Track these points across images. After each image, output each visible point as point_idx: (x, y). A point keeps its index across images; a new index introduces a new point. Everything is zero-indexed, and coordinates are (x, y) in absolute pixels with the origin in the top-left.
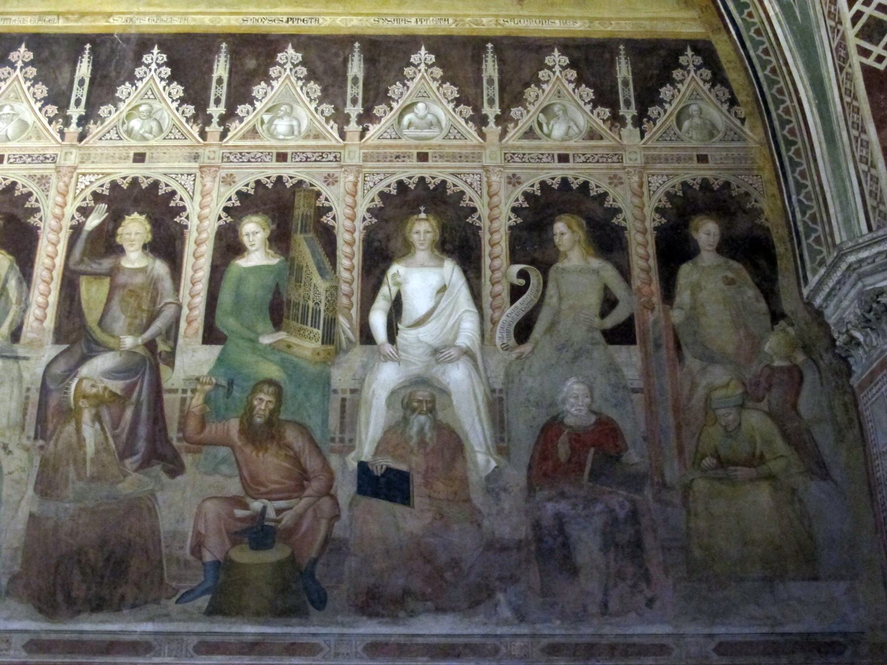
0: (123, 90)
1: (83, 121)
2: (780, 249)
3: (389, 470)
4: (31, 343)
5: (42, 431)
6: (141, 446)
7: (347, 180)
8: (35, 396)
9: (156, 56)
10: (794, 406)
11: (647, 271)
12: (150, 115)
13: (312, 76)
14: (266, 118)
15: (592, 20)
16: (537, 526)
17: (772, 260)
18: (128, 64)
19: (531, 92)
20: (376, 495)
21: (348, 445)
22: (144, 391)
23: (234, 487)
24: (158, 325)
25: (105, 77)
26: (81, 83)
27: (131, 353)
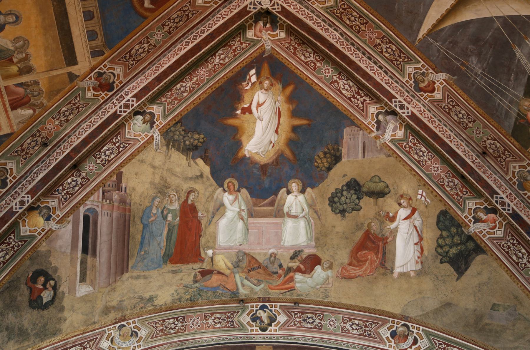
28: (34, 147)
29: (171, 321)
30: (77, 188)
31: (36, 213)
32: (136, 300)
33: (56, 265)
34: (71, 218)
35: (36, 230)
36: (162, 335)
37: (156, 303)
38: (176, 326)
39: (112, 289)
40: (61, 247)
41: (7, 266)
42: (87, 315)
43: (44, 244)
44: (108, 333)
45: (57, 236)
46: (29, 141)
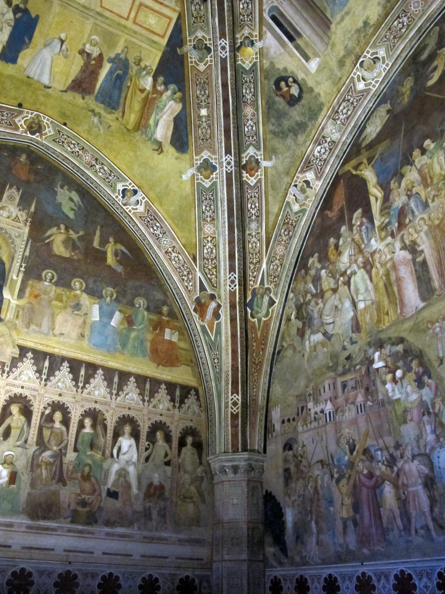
0: (57, 373)
1: (46, 380)
2: (204, 446)
3: (114, 491)
4: (30, 445)
5: (32, 470)
6: (57, 477)
7: (111, 411)
8: (30, 460)
9: (66, 364)
10: (201, 486)
11: (175, 448)
12: (64, 382)
13: (105, 379)
14: (93, 389)
15: (173, 376)
16: (144, 508)
17: (202, 449)
18: (59, 365)
19: (156, 395)
20: (111, 497)
21: (106, 484)
22: (58, 462)
23: (78, 491)
24: (63, 445)
25: (52, 367)
26: (46, 368)
27: (55, 451)
28: (200, 8)
29: (396, 23)
30: (250, 6)
31: (243, 48)
32: (356, 36)
33: (283, 66)
34: (264, 29)
35: (253, 58)
36: (398, 41)
37: (372, 22)
38: (403, 23)
39: (332, 46)
40: (275, 53)
41: (257, 96)
42: (330, 78)
43: (265, 61)
44: (355, 77)
45: (267, 48)
46: (193, 8)
